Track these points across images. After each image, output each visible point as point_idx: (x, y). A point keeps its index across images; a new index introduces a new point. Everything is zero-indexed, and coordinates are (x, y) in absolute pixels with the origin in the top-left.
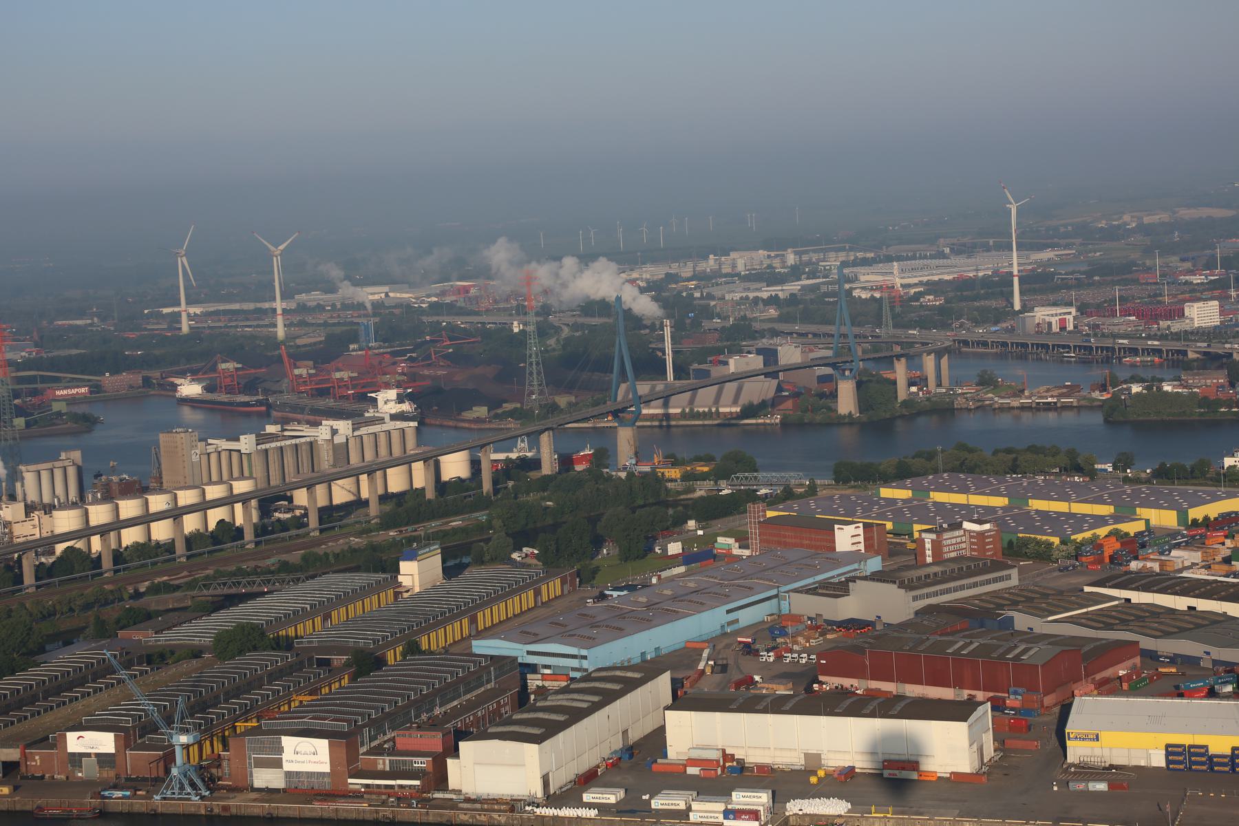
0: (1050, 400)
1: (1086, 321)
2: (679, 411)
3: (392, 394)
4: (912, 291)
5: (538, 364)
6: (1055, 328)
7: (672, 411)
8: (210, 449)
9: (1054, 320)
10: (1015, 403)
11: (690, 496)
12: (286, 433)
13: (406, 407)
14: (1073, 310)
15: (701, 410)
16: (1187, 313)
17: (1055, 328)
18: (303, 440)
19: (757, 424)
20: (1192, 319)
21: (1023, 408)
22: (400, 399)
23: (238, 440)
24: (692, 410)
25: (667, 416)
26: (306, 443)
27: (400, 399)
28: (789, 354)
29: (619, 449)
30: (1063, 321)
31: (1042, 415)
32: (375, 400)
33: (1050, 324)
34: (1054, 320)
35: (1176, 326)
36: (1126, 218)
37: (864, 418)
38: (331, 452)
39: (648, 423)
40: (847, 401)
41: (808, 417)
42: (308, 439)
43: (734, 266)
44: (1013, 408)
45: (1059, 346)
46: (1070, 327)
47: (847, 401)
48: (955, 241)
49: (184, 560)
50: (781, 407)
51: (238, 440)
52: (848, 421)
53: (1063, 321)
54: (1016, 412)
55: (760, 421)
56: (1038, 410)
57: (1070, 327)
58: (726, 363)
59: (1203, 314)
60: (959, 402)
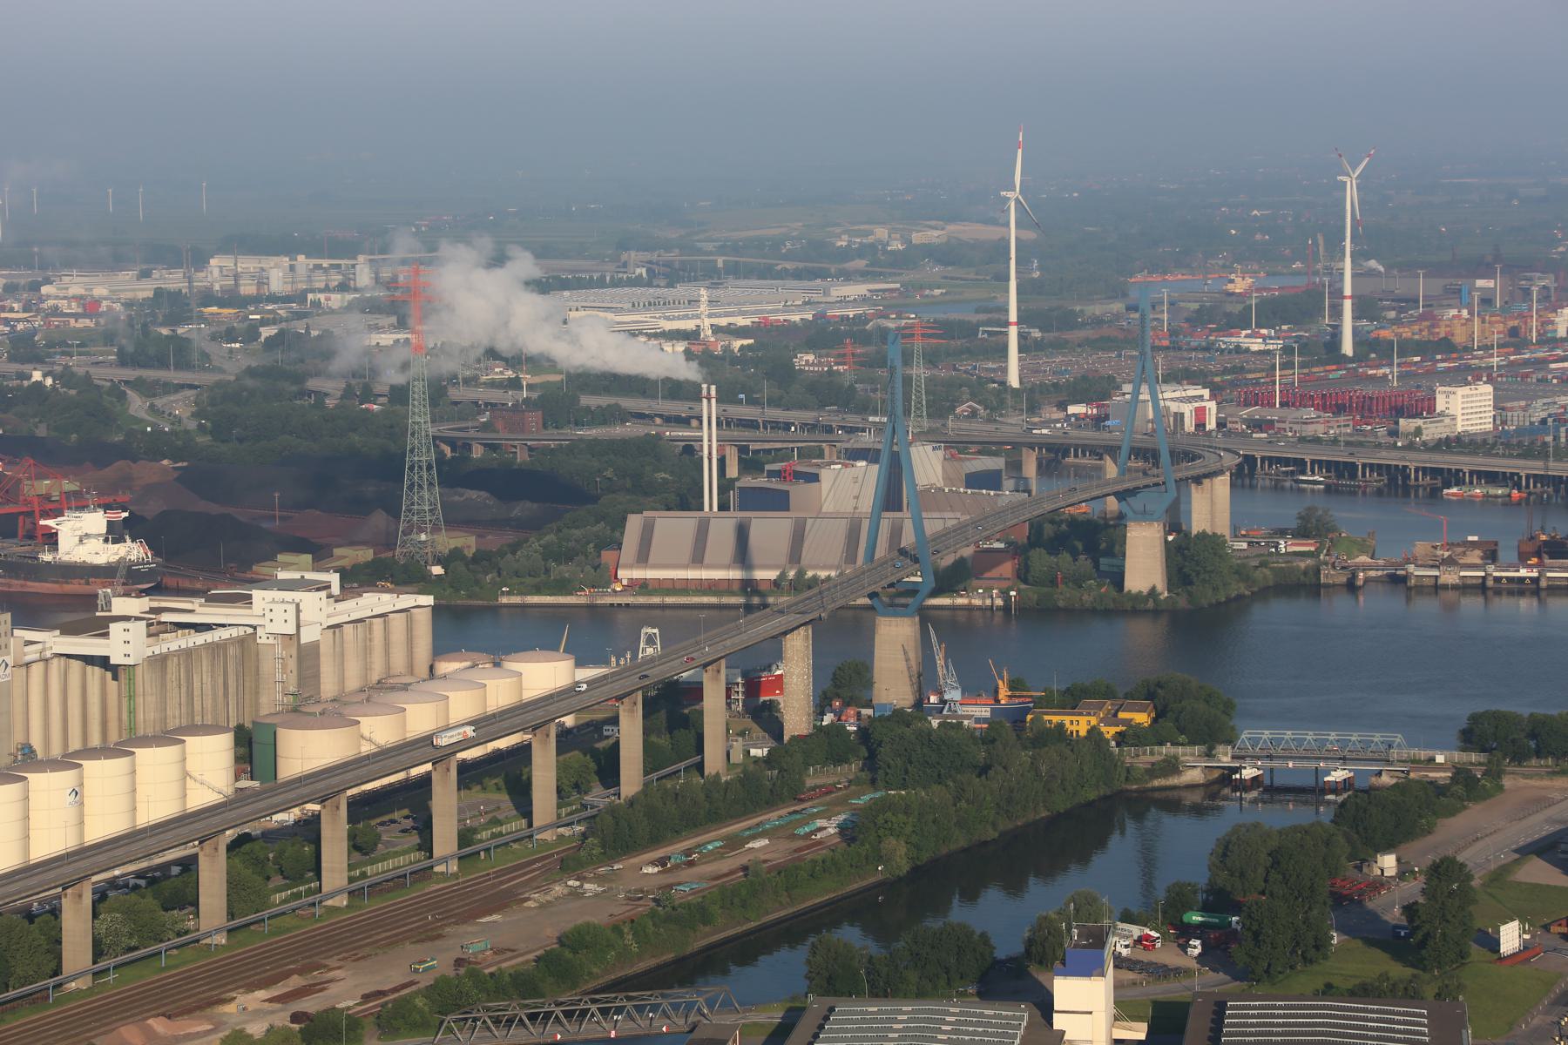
0: (1523, 573)
1: (1245, 412)
2: (772, 575)
3: (96, 521)
4: (737, 344)
5: (429, 468)
6: (1189, 425)
7: (760, 575)
8: (31, 653)
9: (1187, 410)
10: (1450, 577)
11: (1173, 781)
12: (166, 617)
13: (132, 551)
14: (1206, 393)
15: (823, 574)
16: (1439, 408)
17: (1189, 425)
18: (224, 634)
19: (953, 608)
20: (1454, 418)
21: (1464, 588)
22: (114, 534)
23: (106, 635)
24: (801, 573)
25: (748, 587)
26: (231, 640)
27: (114, 534)
28: (928, 465)
29: (877, 664)
30: (1200, 412)
31: (1504, 604)
32: (52, 539)
33: (1179, 417)
34: (1187, 410)
35: (1432, 431)
36: (881, 233)
37: (1182, 603)
38: (292, 664)
39: (713, 600)
40: (1144, 564)
41: (1064, 595)
42: (234, 632)
43: (262, 281)
44: (1445, 587)
45: (1270, 459)
46: (1211, 425)
47: (1144, 564)
48: (655, 257)
49: (221, 939)
50: (987, 575)
51: (106, 635)
52: (1142, 607)
53: (1200, 412)
54: (1451, 595)
55: (960, 601)
56: (1498, 592)
57: (1211, 425)
58: (815, 478)
59: (1467, 408)
60: (1328, 576)
